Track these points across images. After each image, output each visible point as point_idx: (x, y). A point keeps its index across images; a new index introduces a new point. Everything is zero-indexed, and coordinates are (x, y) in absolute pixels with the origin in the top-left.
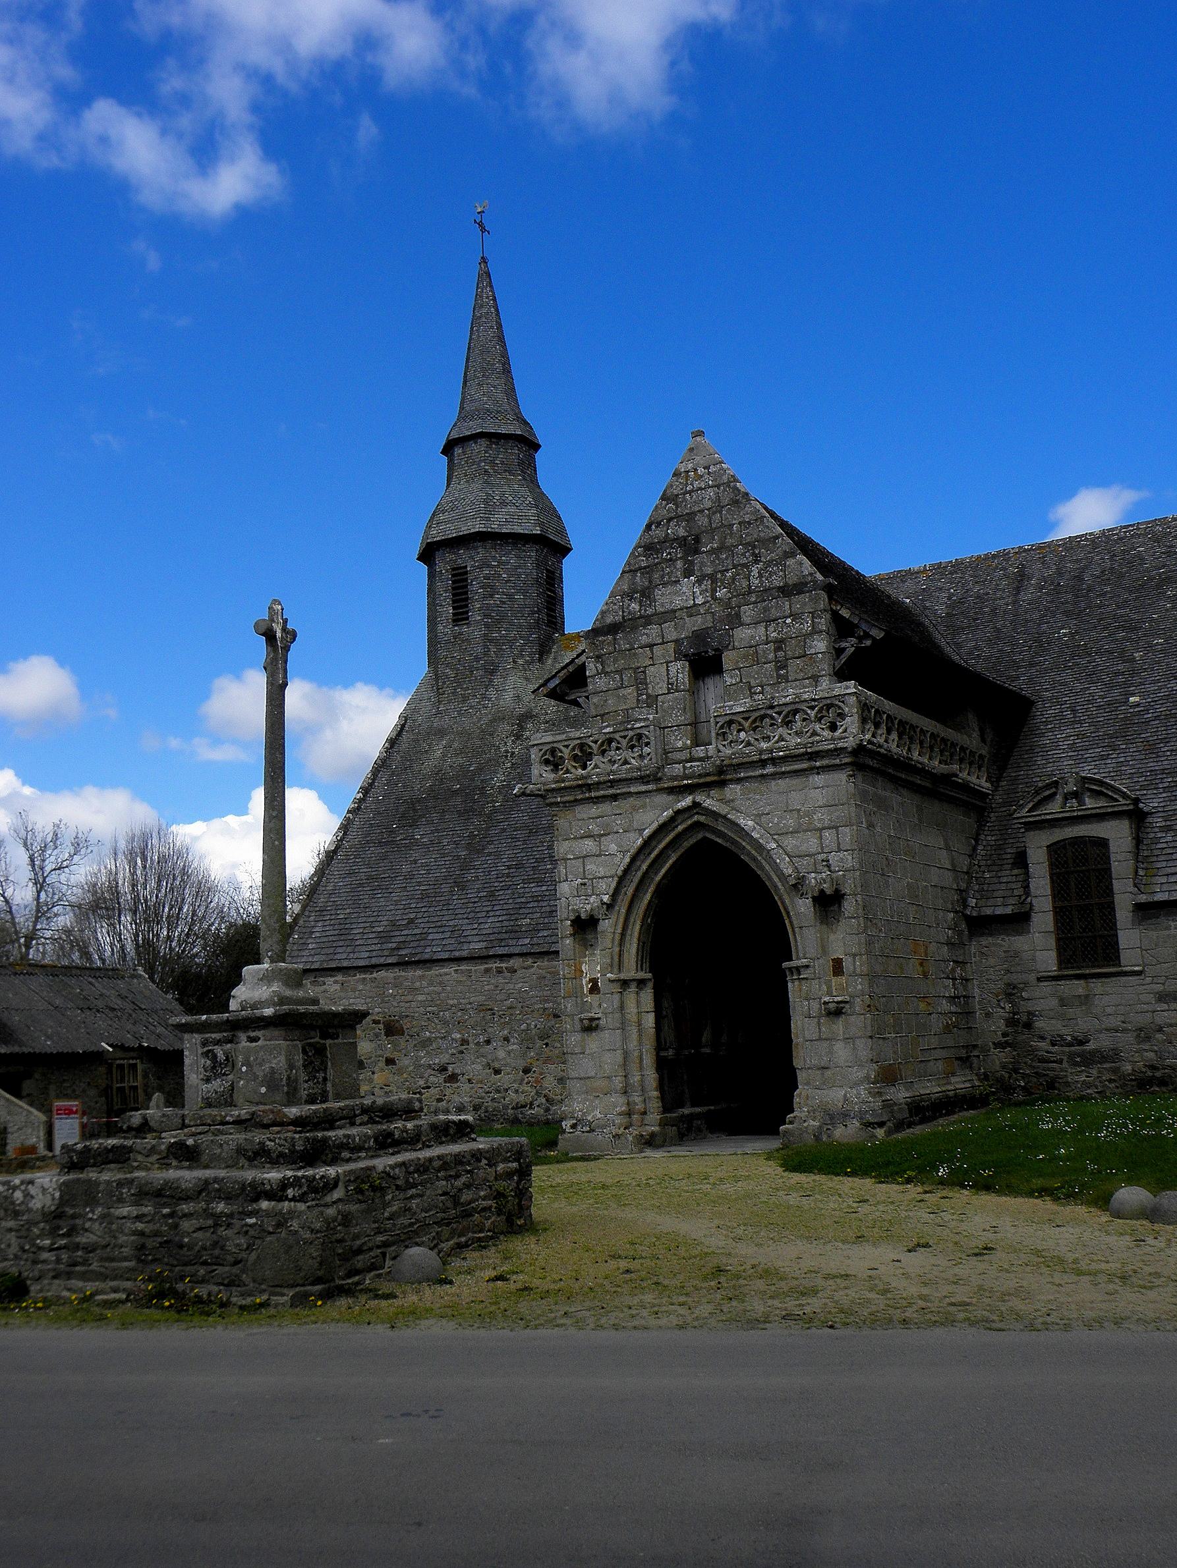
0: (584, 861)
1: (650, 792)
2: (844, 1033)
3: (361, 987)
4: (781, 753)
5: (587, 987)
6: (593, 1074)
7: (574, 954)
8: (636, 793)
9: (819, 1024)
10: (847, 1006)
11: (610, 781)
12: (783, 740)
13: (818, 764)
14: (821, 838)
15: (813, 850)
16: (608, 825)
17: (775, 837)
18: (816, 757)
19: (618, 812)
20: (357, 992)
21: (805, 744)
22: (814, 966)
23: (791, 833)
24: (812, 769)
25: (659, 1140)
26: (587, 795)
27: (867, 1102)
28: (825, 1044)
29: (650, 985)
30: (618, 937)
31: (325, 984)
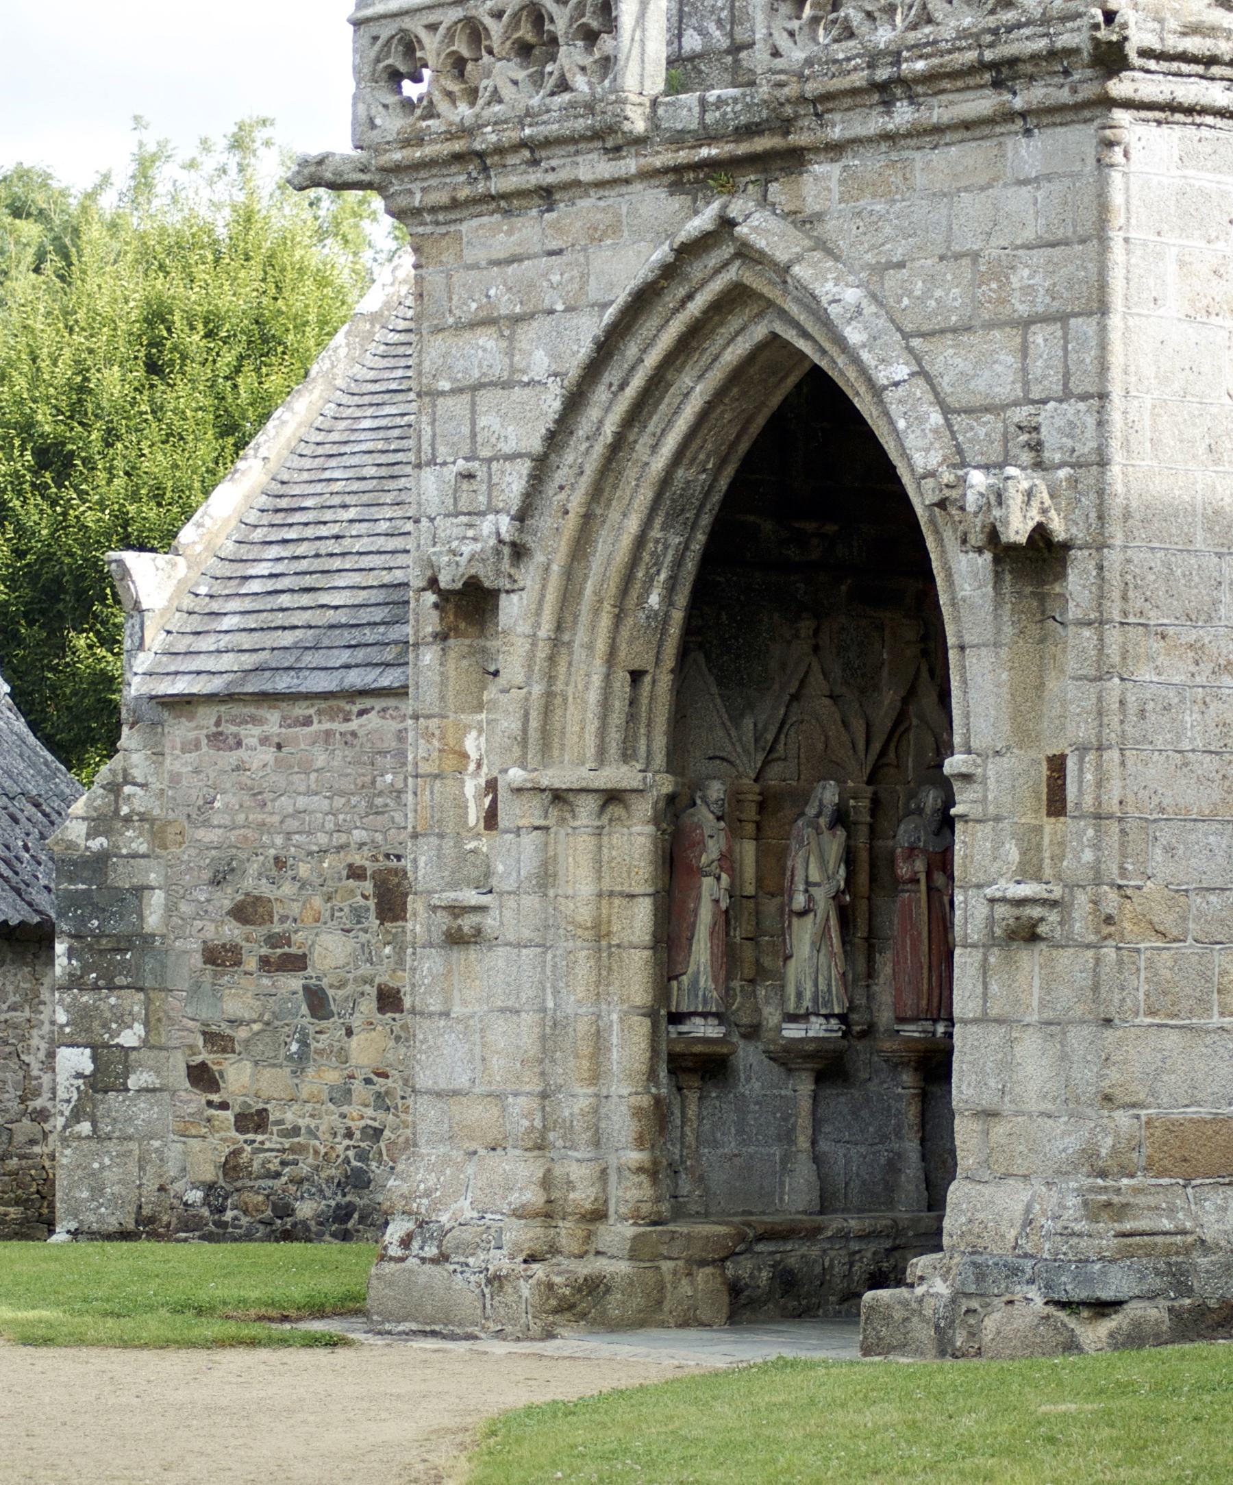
0: (473, 404)
1: (627, 181)
2: (1042, 1005)
3: (321, 760)
4: (920, 65)
5: (479, 805)
6: (462, 1082)
7: (442, 698)
8: (600, 184)
9: (985, 967)
10: (1053, 917)
11: (523, 144)
12: (930, 21)
13: (1018, 103)
14: (1024, 350)
15: (1007, 389)
16: (532, 285)
17: (916, 342)
18: (1014, 79)
19: (554, 245)
20: (313, 776)
21: (977, 36)
22: (985, 778)
23: (954, 330)
24: (1009, 116)
25: (614, 1305)
26: (481, 188)
27: (1073, 1234)
28: (996, 1036)
29: (644, 808)
30: (542, 652)
31: (239, 744)
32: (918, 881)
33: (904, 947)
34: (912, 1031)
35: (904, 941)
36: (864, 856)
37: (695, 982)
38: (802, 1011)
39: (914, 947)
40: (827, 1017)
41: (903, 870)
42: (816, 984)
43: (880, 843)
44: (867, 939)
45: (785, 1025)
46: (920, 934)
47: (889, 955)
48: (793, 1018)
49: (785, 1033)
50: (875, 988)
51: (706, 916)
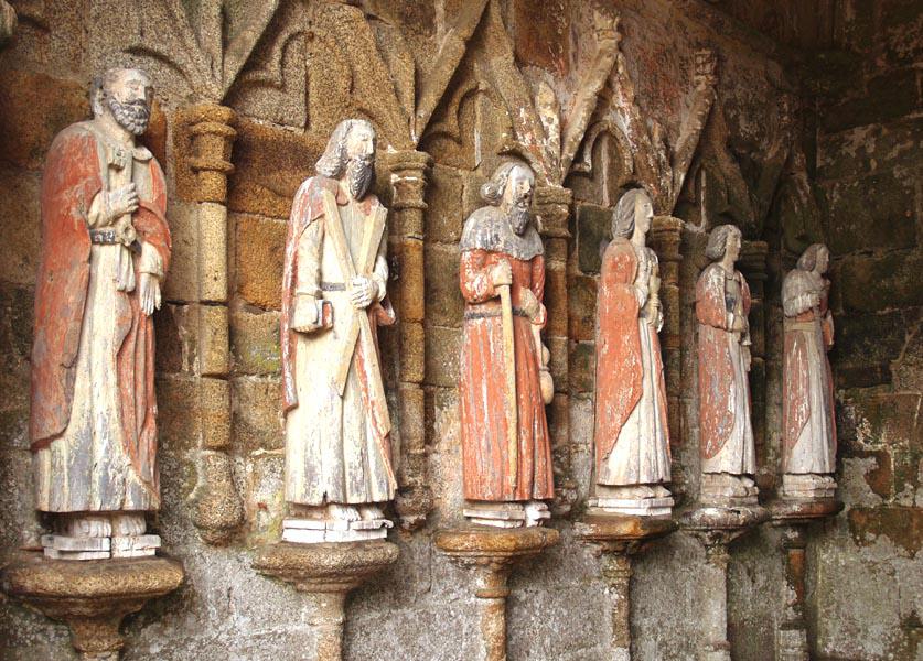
32: (498, 299)
33: (478, 397)
34: (489, 517)
35: (477, 388)
36: (415, 257)
37: (84, 454)
38: (317, 500)
39: (493, 396)
40: (358, 507)
41: (474, 283)
42: (341, 455)
43: (438, 247)
44: (422, 384)
45: (287, 523)
46: (502, 378)
47: (454, 408)
48: (304, 510)
49: (290, 536)
50: (435, 458)
51: (104, 319)
